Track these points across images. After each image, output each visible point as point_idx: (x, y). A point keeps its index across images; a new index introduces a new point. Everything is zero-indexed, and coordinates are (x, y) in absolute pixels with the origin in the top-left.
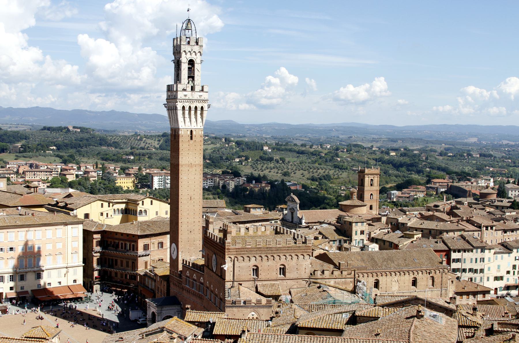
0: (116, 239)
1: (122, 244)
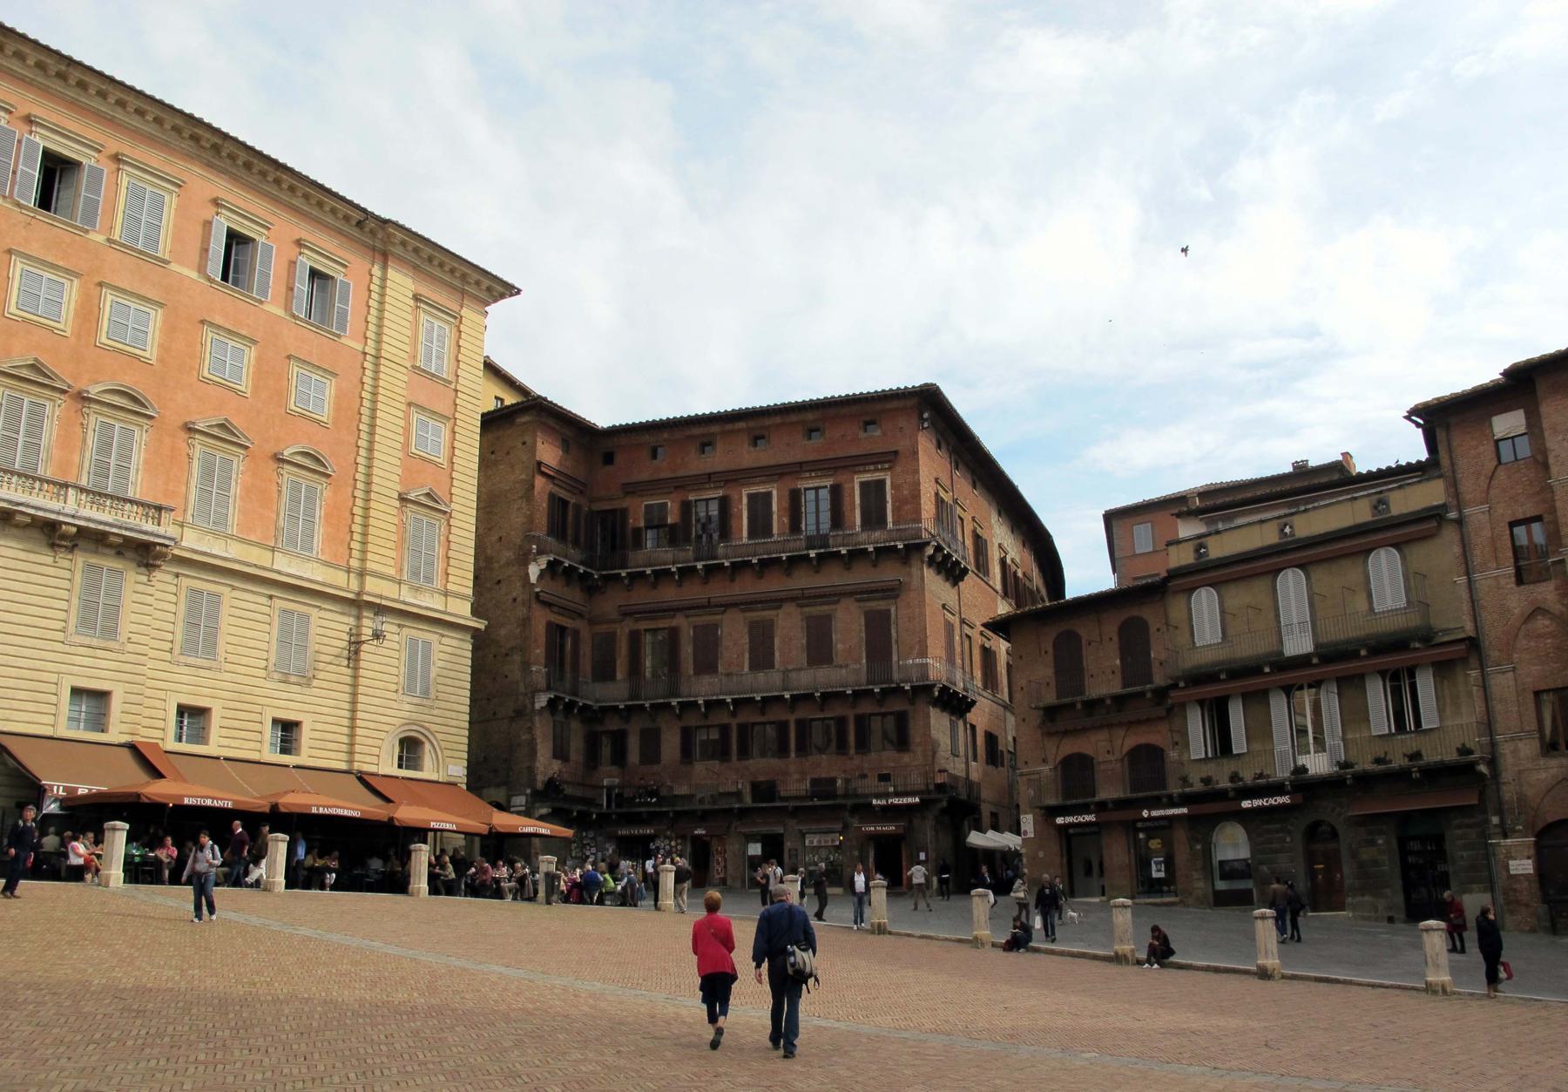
0: (709, 478)
1: (760, 504)
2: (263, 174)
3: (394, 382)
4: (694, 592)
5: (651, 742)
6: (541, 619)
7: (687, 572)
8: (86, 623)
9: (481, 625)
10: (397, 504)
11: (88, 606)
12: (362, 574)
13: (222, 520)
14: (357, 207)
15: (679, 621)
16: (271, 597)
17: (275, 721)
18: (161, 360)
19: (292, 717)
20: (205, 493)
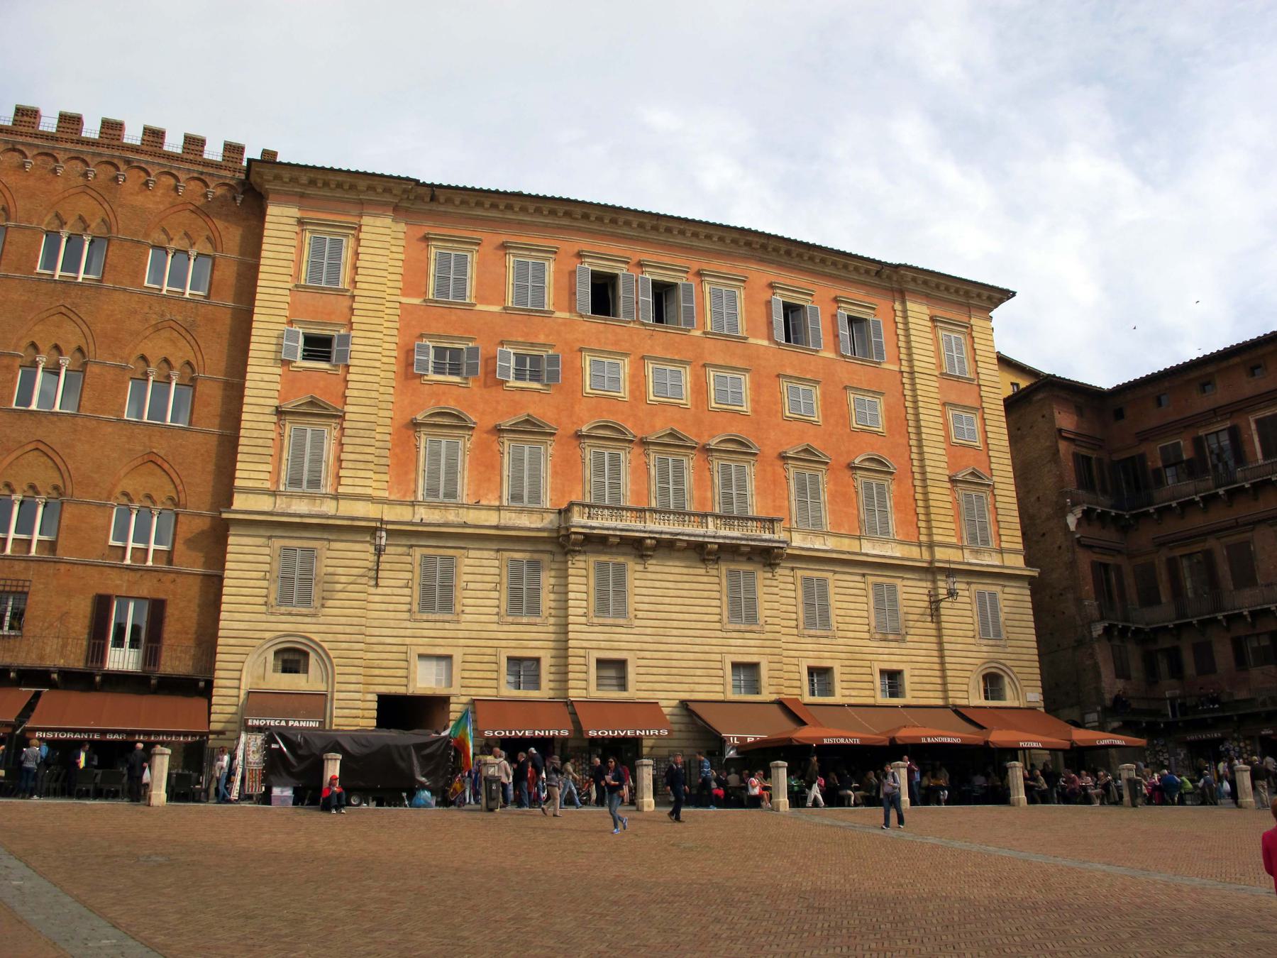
2: (800, 256)
3: (929, 389)
4: (1220, 515)
5: (1204, 654)
6: (1085, 560)
7: (1210, 499)
8: (735, 613)
9: (1034, 573)
10: (949, 485)
11: (734, 603)
12: (931, 546)
13: (818, 521)
14: (873, 261)
15: (1211, 543)
16: (864, 575)
17: (882, 672)
18: (754, 411)
19: (895, 667)
20: (802, 504)
